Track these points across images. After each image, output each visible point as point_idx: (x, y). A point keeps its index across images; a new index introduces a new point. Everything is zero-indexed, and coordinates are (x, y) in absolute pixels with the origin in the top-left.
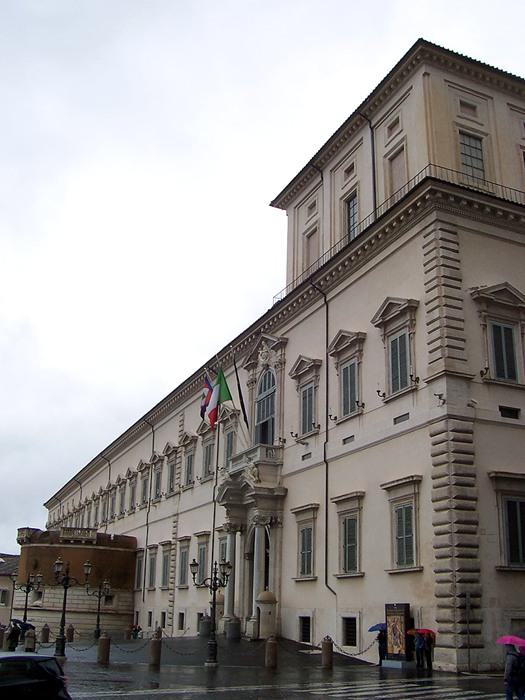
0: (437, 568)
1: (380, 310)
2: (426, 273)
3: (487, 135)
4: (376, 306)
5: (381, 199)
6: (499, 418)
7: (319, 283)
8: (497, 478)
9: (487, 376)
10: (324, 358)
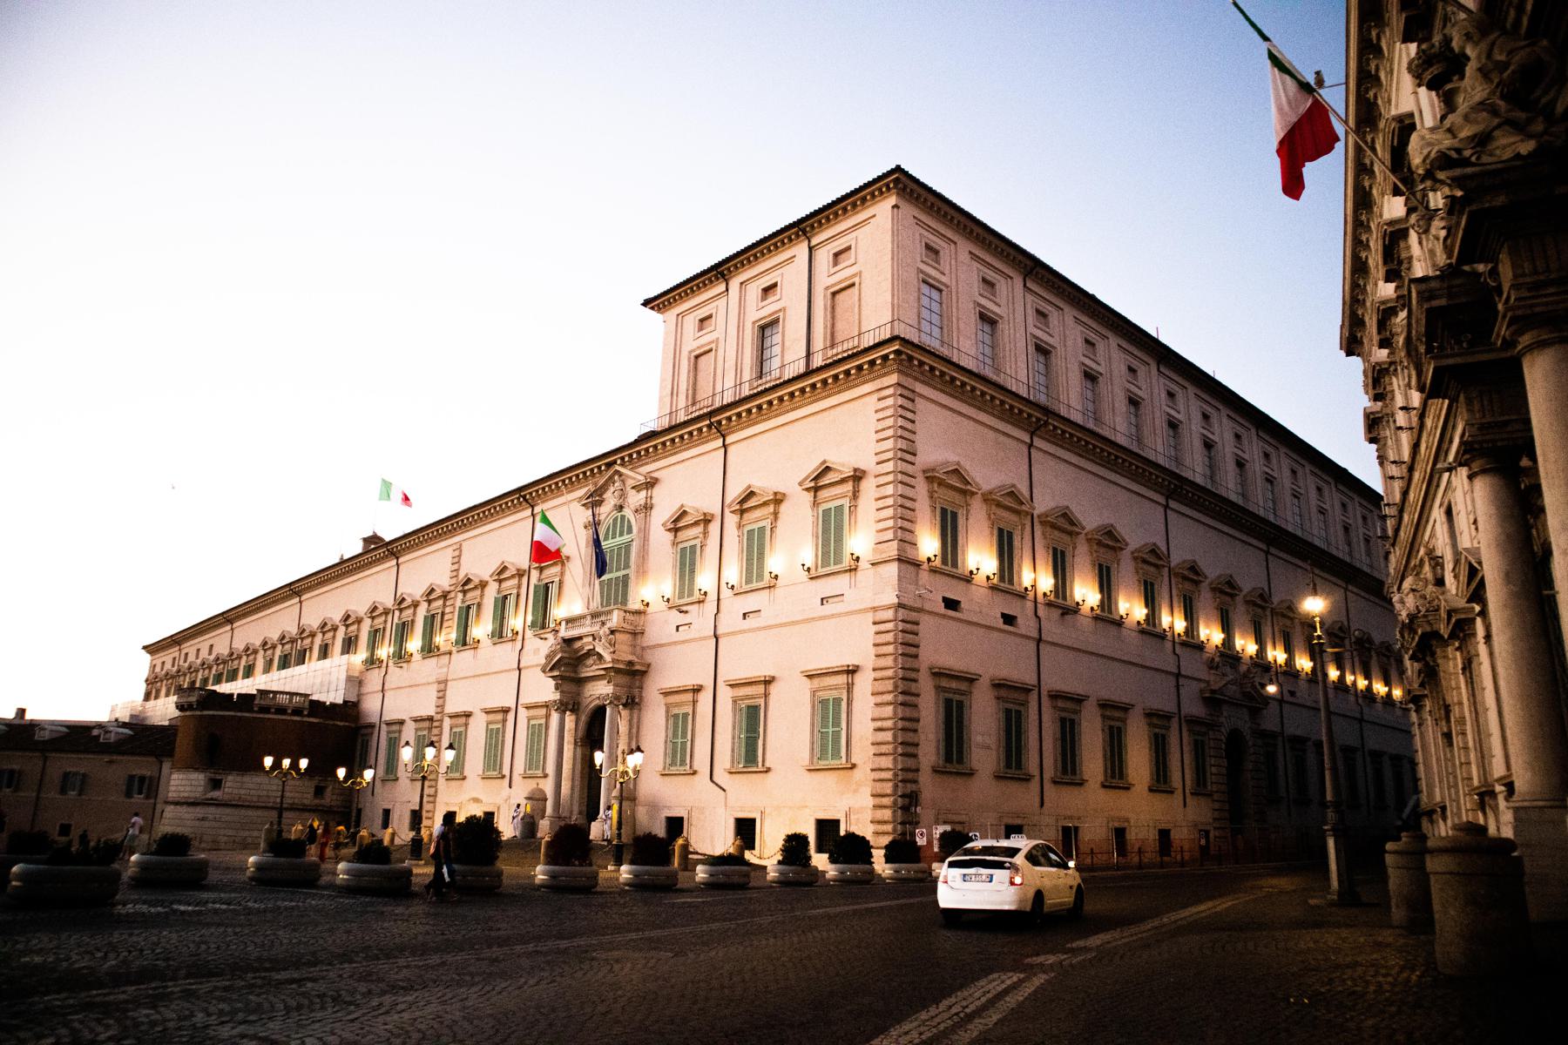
1: (813, 472)
2: (877, 441)
3: (947, 287)
4: (811, 466)
5: (819, 342)
7: (719, 422)
8: (938, 674)
9: (933, 564)
10: (717, 510)
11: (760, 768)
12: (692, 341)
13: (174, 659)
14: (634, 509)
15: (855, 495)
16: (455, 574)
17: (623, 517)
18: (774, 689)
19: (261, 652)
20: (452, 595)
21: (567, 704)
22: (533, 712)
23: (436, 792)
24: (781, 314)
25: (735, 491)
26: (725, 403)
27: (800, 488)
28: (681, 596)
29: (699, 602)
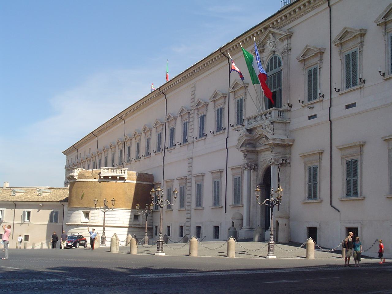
11: (359, 198)
13: (76, 156)
14: (281, 52)
16: (193, 100)
17: (276, 57)
18: (366, 149)
19: (110, 150)
20: (192, 111)
21: (251, 165)
22: (235, 171)
23: (191, 216)
25: (336, 33)
28: (310, 99)
29: (320, 101)
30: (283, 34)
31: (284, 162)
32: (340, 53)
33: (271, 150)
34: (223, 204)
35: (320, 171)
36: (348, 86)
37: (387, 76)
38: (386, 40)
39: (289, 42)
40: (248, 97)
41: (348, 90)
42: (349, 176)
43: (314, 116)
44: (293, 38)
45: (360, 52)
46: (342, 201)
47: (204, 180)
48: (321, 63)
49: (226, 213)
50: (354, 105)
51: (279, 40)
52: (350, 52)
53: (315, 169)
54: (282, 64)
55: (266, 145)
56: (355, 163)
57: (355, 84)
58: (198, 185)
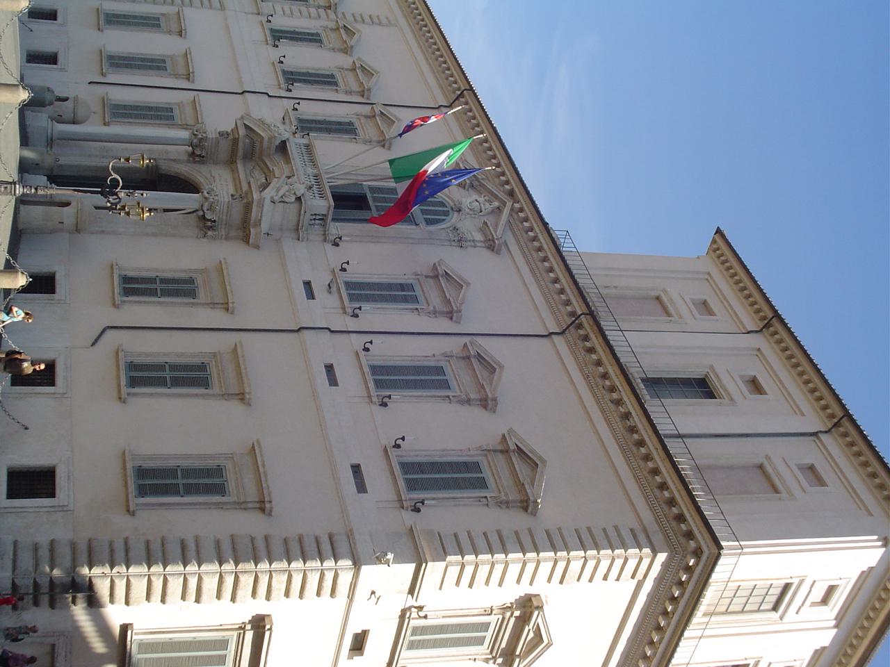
0: (131, 542)
6: (354, 628)
9: (414, 615)
11: (124, 390)
12: (680, 295)
14: (459, 225)
15: (505, 504)
16: (359, 18)
17: (446, 213)
18: (235, 406)
20: (333, 16)
21: (203, 148)
22: (189, 109)
24: (726, 401)
25: (493, 348)
26: (607, 333)
27: (505, 432)
28: (349, 285)
30: (496, 232)
31: (209, 224)
32: (449, 354)
33: (237, 196)
34: (112, 78)
35: (187, 304)
36: (375, 370)
37: (393, 453)
38: (472, 453)
39: (478, 244)
40: (360, 147)
41: (367, 370)
42: (174, 367)
43: (310, 295)
44: (486, 253)
45: (448, 397)
46: (117, 353)
47: (170, 35)
48: (429, 313)
49: (90, 83)
50: (333, 381)
51: (485, 223)
52: (449, 376)
53: (192, 293)
54: (431, 228)
55: (249, 183)
56: (204, 382)
57: (379, 384)
58: (158, 19)
